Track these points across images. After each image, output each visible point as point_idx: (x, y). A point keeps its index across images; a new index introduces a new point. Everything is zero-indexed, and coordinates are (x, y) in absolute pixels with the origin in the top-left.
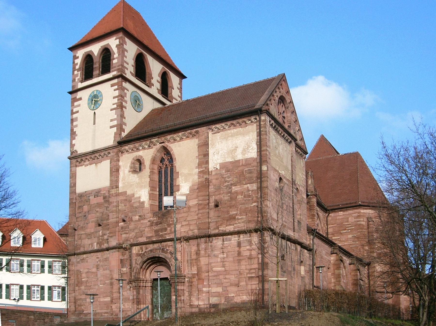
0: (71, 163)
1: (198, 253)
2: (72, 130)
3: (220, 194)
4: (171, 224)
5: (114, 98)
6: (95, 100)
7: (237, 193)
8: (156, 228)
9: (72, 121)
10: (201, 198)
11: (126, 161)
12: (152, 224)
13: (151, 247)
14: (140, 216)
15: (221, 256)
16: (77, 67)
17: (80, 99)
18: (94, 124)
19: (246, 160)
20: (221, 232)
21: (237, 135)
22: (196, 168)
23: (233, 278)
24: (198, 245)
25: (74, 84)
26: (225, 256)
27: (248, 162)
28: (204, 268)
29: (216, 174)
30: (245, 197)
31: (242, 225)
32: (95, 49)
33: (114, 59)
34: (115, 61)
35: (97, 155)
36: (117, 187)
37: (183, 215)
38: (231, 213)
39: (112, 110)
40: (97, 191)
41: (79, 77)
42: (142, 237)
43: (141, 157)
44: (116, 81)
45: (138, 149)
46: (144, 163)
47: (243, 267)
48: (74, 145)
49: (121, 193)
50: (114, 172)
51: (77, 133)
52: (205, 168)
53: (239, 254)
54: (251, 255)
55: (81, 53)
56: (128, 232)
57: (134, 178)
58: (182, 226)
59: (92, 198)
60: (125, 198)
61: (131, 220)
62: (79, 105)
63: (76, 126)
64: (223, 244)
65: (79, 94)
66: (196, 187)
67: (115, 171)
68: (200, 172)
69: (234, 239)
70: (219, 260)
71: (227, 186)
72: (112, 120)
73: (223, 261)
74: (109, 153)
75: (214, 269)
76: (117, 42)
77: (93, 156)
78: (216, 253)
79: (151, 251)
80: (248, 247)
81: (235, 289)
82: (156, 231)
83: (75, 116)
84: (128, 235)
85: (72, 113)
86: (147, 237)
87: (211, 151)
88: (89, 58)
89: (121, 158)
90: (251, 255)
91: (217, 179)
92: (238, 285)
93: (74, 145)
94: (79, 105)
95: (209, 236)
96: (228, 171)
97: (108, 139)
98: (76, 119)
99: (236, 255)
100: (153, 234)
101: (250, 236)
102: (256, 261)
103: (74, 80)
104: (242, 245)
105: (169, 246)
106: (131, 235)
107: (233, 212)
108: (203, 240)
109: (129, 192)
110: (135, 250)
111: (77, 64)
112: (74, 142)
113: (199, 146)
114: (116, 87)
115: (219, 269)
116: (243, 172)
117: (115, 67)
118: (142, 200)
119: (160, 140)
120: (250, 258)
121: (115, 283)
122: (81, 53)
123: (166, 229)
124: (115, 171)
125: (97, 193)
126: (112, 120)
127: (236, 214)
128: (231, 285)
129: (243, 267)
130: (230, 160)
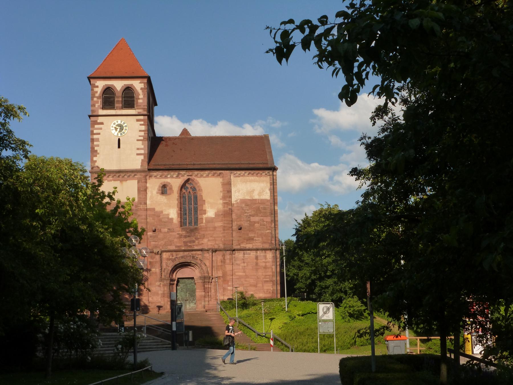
1: (223, 261)
2: (93, 148)
3: (241, 221)
4: (198, 238)
5: (140, 131)
7: (255, 222)
8: (185, 240)
10: (226, 222)
11: (154, 184)
12: (181, 236)
13: (181, 254)
14: (168, 229)
15: (243, 265)
16: (97, 95)
17: (102, 123)
18: (119, 147)
19: (262, 200)
20: (242, 248)
21: (254, 181)
22: (221, 199)
23: (252, 281)
24: (224, 256)
25: (93, 108)
26: (246, 264)
27: (263, 202)
28: (229, 273)
29: (238, 206)
30: (261, 225)
31: (259, 244)
32: (119, 85)
33: (139, 99)
34: (140, 101)
35: (122, 175)
36: (146, 204)
37: (209, 232)
38: (250, 235)
39: (138, 140)
41: (99, 104)
42: (171, 245)
43: (169, 183)
44: (142, 117)
45: (166, 177)
47: (260, 274)
48: (96, 161)
49: (149, 209)
51: (98, 152)
52: (229, 201)
53: (257, 264)
54: (266, 265)
55: (101, 85)
57: (163, 199)
58: (209, 240)
60: (153, 213)
61: (160, 231)
62: (101, 129)
63: (98, 146)
64: (244, 257)
65: (100, 119)
66: (221, 214)
67: (143, 191)
68: (224, 203)
69: (253, 254)
70: (241, 267)
71: (247, 216)
72: (138, 149)
73: (244, 269)
74: (135, 175)
75: (237, 274)
77: (118, 175)
78: (238, 262)
79: (182, 257)
80: (264, 260)
81: (253, 288)
82: (184, 242)
83: (95, 137)
84: (157, 243)
86: (176, 246)
87: (233, 190)
88: (108, 91)
89: (148, 181)
90: (266, 265)
91: (238, 210)
92: (255, 286)
93: (96, 161)
94: (101, 129)
96: (247, 205)
98: (98, 140)
99: (254, 265)
100: (182, 244)
101: (265, 253)
102: (270, 270)
103: (93, 105)
104: (259, 258)
105: (198, 255)
106: (160, 243)
107: (251, 235)
108: (228, 252)
109: (158, 209)
110: (165, 255)
111: (97, 92)
112: (95, 159)
113: (223, 184)
114: (142, 123)
115: (241, 274)
116: (259, 208)
117: (140, 106)
118: (170, 217)
120: (265, 268)
122: (101, 85)
123: (194, 242)
124: (143, 191)
126: (138, 149)
127: (254, 237)
128: (251, 285)
129: (260, 274)
130: (248, 198)
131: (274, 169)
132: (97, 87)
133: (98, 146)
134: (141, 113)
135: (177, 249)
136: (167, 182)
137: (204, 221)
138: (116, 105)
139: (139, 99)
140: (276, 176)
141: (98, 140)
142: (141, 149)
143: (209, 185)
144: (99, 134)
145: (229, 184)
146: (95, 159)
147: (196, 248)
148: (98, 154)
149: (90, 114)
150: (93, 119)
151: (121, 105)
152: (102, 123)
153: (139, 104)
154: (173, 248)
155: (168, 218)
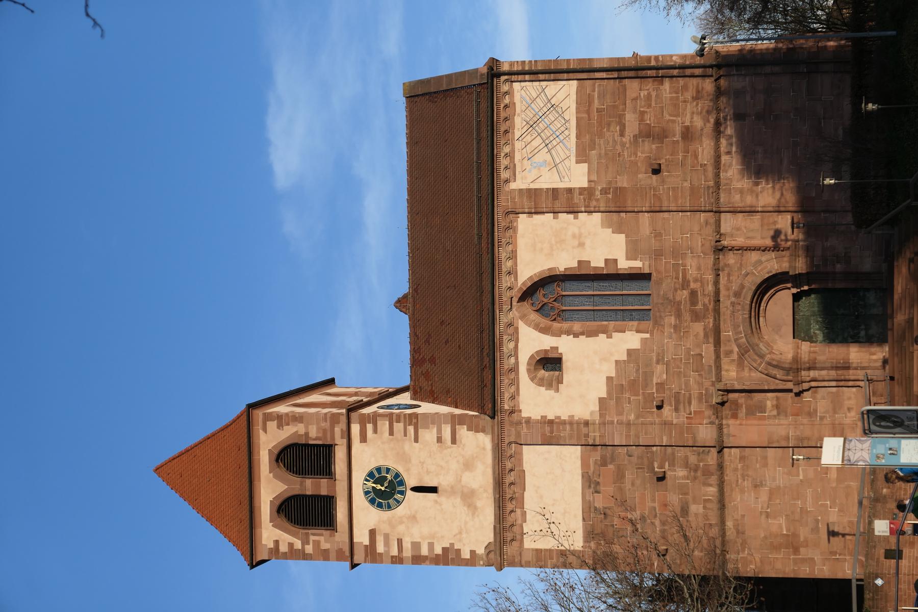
0: (512, 564)
6: (386, 489)
9: (417, 559)
11: (533, 400)
14: (658, 363)
27: (584, 103)
32: (270, 488)
33: (307, 434)
36: (587, 423)
38: (678, 138)
39: (416, 440)
40: (588, 484)
41: (322, 539)
43: (532, 357)
44: (355, 429)
46: (546, 351)
48: (473, 552)
50: (552, 432)
52: (580, 194)
55: (270, 533)
56: (687, 395)
59: (599, 502)
62: (387, 537)
63: (431, 546)
65: (361, 537)
67: (552, 432)
72: (439, 440)
76: (272, 425)
80: (748, 98)
83: (407, 553)
85: (398, 560)
93: (473, 552)
95: (718, 185)
96: (592, 146)
97: (478, 444)
98: (416, 546)
111: (291, 545)
112: (466, 555)
114: (370, 427)
117: (325, 431)
118: (624, 357)
119: (506, 307)
121: (798, 433)
122: (270, 533)
124: (552, 432)
125: (590, 482)
131: (494, 71)
132: (277, 542)
133: (431, 546)
134: (345, 427)
135: (711, 340)
136: (528, 364)
137: (637, 264)
138: (324, 492)
139: (307, 434)
140: (512, 64)
141: (416, 546)
142: (439, 431)
143: (538, 247)
144: (400, 542)
145: (533, 194)
146: (466, 555)
147: (710, 288)
148: (452, 545)
149: (347, 564)
150: (359, 557)
151: (324, 482)
152: (372, 533)
153: (320, 435)
154: (708, 350)
155: (628, 361)
